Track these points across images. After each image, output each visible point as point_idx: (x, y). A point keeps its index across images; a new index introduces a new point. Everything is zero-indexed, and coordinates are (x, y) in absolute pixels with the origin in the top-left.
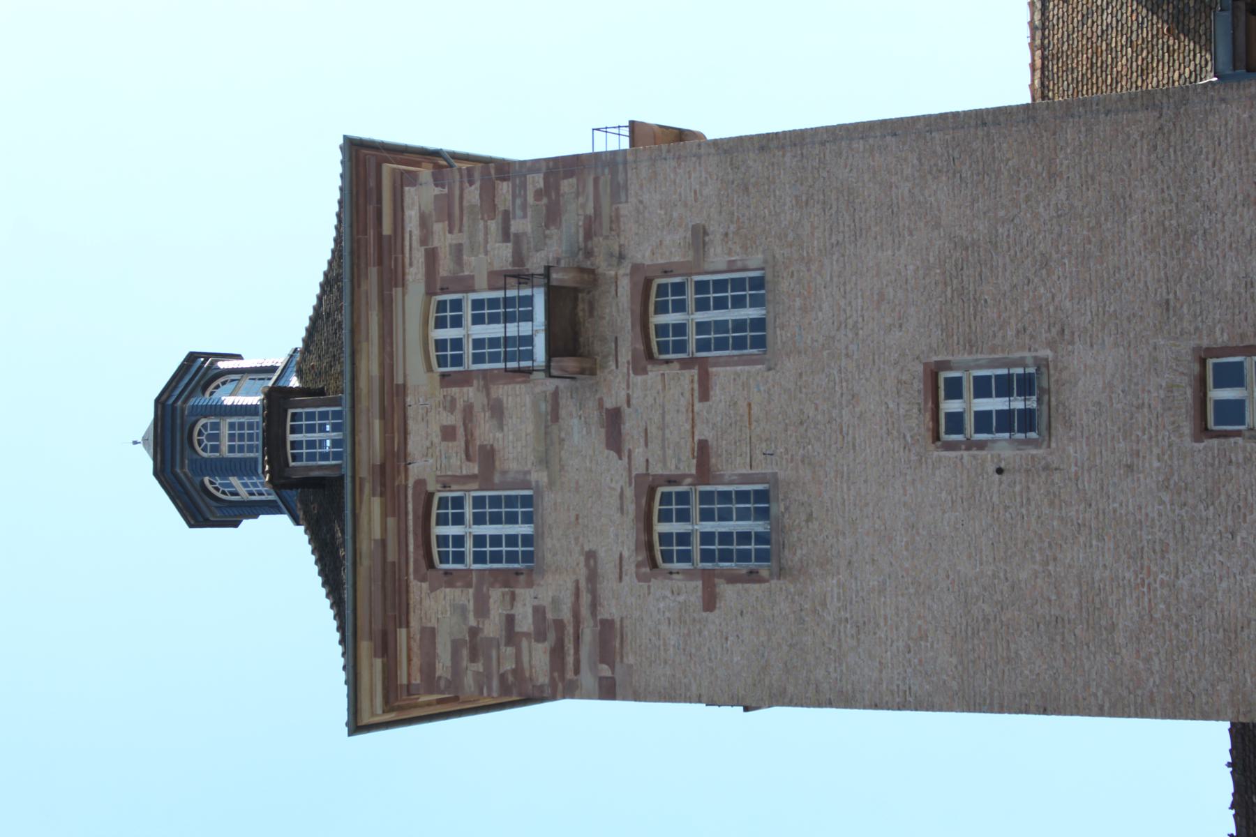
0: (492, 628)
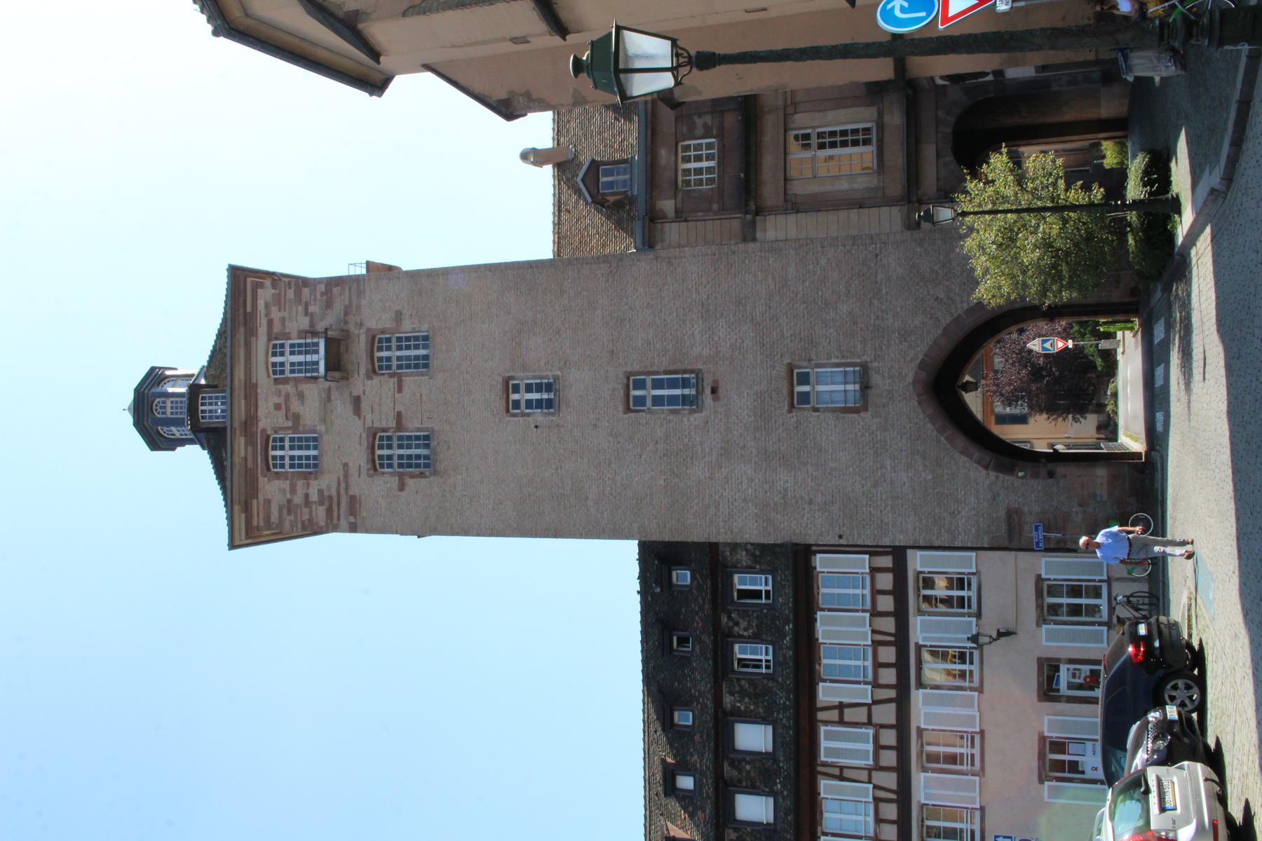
0: (298, 499)
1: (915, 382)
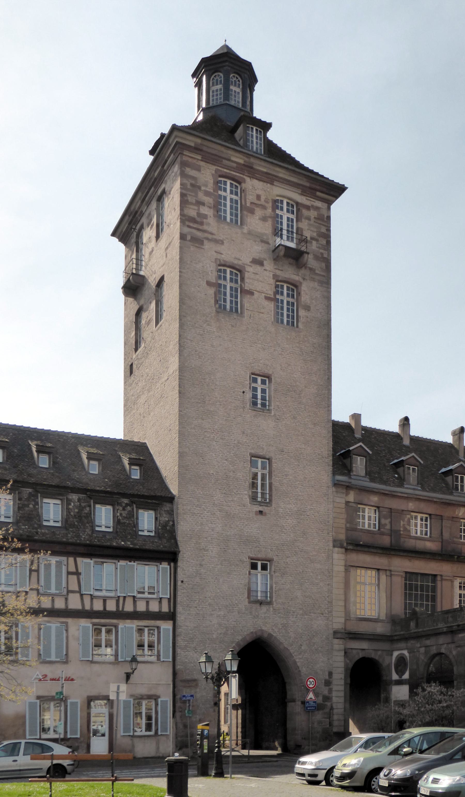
1: (262, 630)
